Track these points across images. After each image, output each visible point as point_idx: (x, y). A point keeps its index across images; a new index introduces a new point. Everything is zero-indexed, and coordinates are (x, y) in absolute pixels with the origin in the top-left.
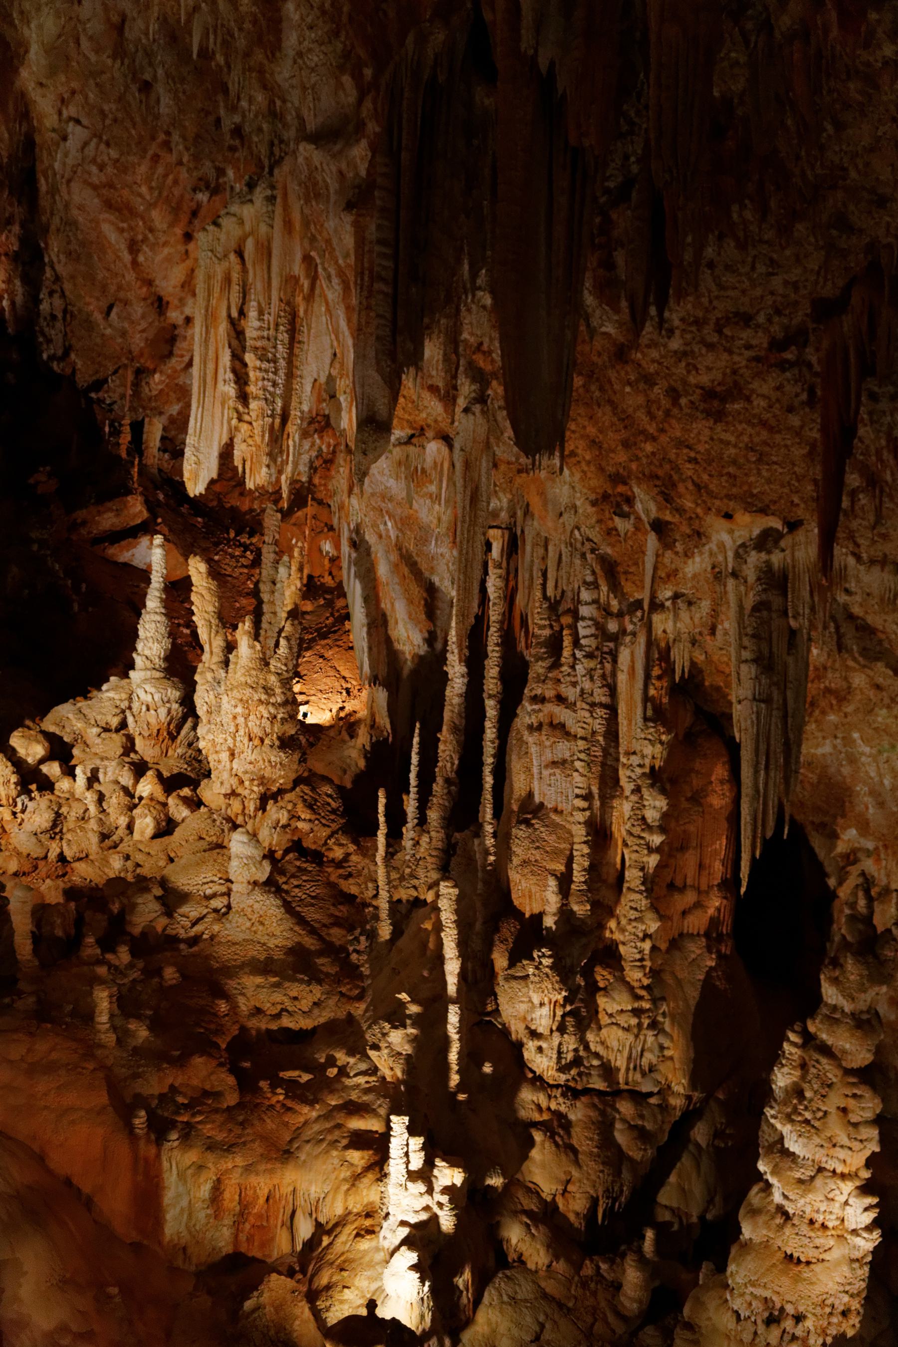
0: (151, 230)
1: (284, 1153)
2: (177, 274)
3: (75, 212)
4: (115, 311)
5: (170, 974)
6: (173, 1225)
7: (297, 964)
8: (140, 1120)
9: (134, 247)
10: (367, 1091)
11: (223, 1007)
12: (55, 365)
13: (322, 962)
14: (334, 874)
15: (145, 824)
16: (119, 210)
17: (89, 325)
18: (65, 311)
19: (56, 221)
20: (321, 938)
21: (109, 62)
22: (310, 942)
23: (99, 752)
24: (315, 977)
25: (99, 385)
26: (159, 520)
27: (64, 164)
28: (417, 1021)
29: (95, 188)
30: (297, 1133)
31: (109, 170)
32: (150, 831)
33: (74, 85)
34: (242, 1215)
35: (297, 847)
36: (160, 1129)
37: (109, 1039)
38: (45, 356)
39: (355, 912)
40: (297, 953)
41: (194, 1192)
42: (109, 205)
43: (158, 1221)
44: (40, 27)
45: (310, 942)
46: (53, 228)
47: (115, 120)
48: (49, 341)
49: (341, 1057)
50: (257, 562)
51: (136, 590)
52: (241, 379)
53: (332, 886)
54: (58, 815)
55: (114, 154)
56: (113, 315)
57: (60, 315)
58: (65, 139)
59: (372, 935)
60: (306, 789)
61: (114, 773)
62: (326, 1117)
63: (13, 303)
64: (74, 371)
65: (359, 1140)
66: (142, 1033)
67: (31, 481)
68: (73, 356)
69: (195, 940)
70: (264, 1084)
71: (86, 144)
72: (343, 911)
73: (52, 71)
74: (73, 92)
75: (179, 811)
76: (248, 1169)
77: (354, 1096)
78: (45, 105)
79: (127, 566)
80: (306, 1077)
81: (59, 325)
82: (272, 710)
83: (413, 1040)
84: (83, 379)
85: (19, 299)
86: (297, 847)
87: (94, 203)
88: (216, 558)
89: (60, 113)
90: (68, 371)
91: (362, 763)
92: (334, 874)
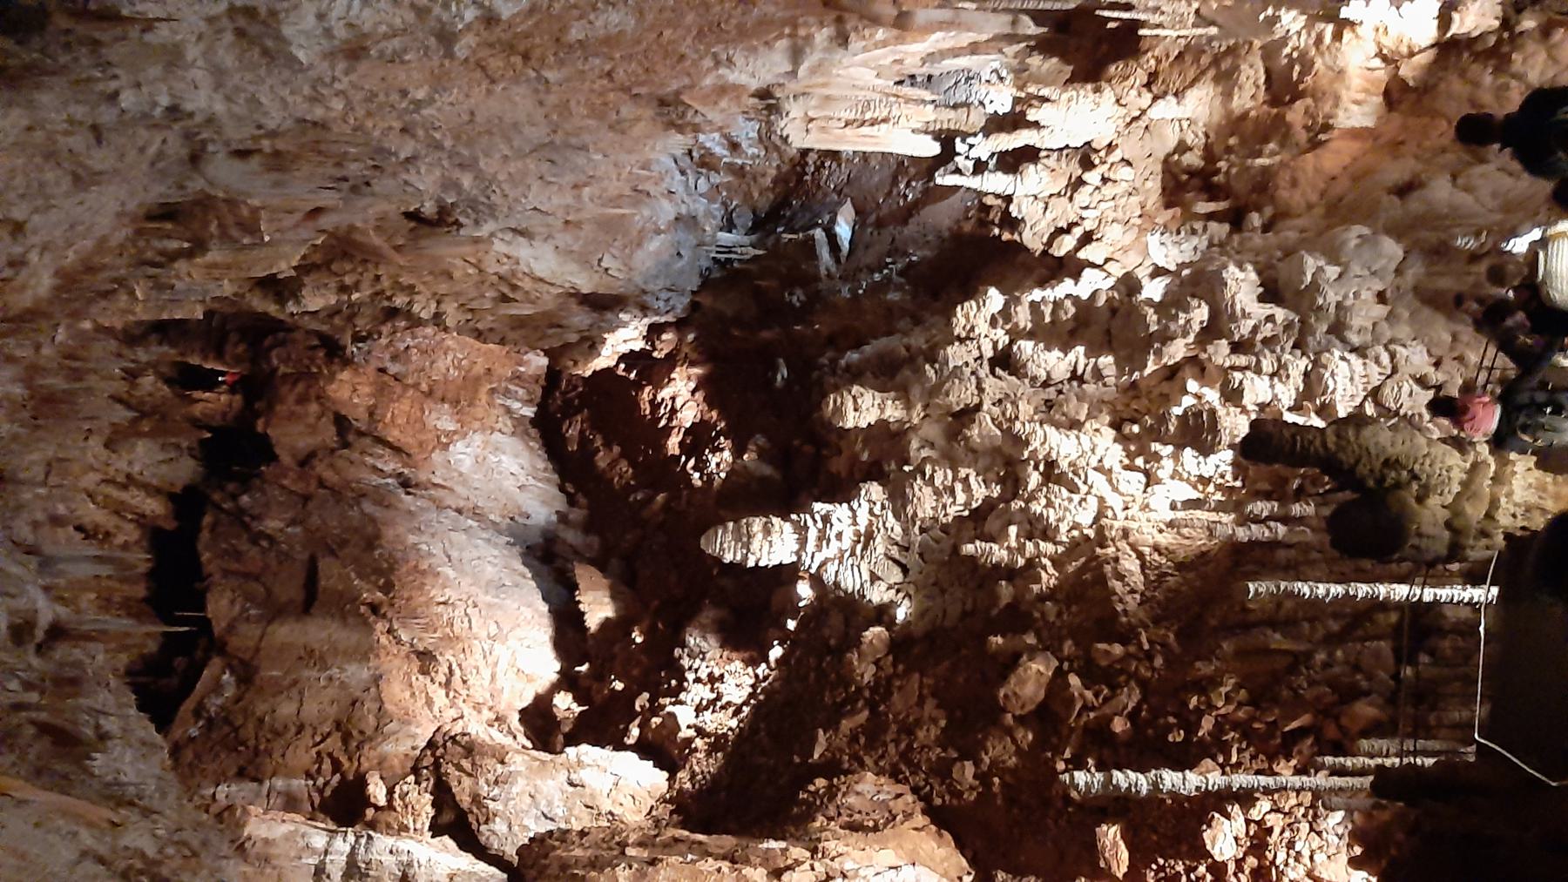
1: (1341, 73)
5: (1232, 141)
6: (1369, 123)
7: (1226, 79)
8: (1322, 137)
9: (658, 232)
10: (1309, 35)
11: (1253, 113)
13: (1225, 65)
14: (1165, 64)
15: (1124, 173)
20: (1208, 69)
22: (1211, 73)
23: (1063, 212)
24: (1235, 68)
28: (1277, 7)
30: (1330, 68)
34: (1366, 91)
35: (1148, 86)
36: (1327, 128)
37: (1278, 158)
39: (1189, 53)
40: (1217, 80)
41: (1356, 110)
43: (1367, 128)
44: (571, 274)
45: (1211, 73)
49: (1287, 50)
50: (835, 155)
53: (1171, 65)
59: (1211, 39)
61: (1083, 196)
62: (1322, 54)
65: (1337, 36)
66: (1272, 146)
69: (1207, 136)
70: (1301, 87)
72: (1188, 58)
75: (1116, 156)
76: (1348, 88)
77: (1311, 42)
80: (1297, 68)
83: (1288, 9)
86: (1148, 86)
91: (1055, 60)
92: (1165, 64)
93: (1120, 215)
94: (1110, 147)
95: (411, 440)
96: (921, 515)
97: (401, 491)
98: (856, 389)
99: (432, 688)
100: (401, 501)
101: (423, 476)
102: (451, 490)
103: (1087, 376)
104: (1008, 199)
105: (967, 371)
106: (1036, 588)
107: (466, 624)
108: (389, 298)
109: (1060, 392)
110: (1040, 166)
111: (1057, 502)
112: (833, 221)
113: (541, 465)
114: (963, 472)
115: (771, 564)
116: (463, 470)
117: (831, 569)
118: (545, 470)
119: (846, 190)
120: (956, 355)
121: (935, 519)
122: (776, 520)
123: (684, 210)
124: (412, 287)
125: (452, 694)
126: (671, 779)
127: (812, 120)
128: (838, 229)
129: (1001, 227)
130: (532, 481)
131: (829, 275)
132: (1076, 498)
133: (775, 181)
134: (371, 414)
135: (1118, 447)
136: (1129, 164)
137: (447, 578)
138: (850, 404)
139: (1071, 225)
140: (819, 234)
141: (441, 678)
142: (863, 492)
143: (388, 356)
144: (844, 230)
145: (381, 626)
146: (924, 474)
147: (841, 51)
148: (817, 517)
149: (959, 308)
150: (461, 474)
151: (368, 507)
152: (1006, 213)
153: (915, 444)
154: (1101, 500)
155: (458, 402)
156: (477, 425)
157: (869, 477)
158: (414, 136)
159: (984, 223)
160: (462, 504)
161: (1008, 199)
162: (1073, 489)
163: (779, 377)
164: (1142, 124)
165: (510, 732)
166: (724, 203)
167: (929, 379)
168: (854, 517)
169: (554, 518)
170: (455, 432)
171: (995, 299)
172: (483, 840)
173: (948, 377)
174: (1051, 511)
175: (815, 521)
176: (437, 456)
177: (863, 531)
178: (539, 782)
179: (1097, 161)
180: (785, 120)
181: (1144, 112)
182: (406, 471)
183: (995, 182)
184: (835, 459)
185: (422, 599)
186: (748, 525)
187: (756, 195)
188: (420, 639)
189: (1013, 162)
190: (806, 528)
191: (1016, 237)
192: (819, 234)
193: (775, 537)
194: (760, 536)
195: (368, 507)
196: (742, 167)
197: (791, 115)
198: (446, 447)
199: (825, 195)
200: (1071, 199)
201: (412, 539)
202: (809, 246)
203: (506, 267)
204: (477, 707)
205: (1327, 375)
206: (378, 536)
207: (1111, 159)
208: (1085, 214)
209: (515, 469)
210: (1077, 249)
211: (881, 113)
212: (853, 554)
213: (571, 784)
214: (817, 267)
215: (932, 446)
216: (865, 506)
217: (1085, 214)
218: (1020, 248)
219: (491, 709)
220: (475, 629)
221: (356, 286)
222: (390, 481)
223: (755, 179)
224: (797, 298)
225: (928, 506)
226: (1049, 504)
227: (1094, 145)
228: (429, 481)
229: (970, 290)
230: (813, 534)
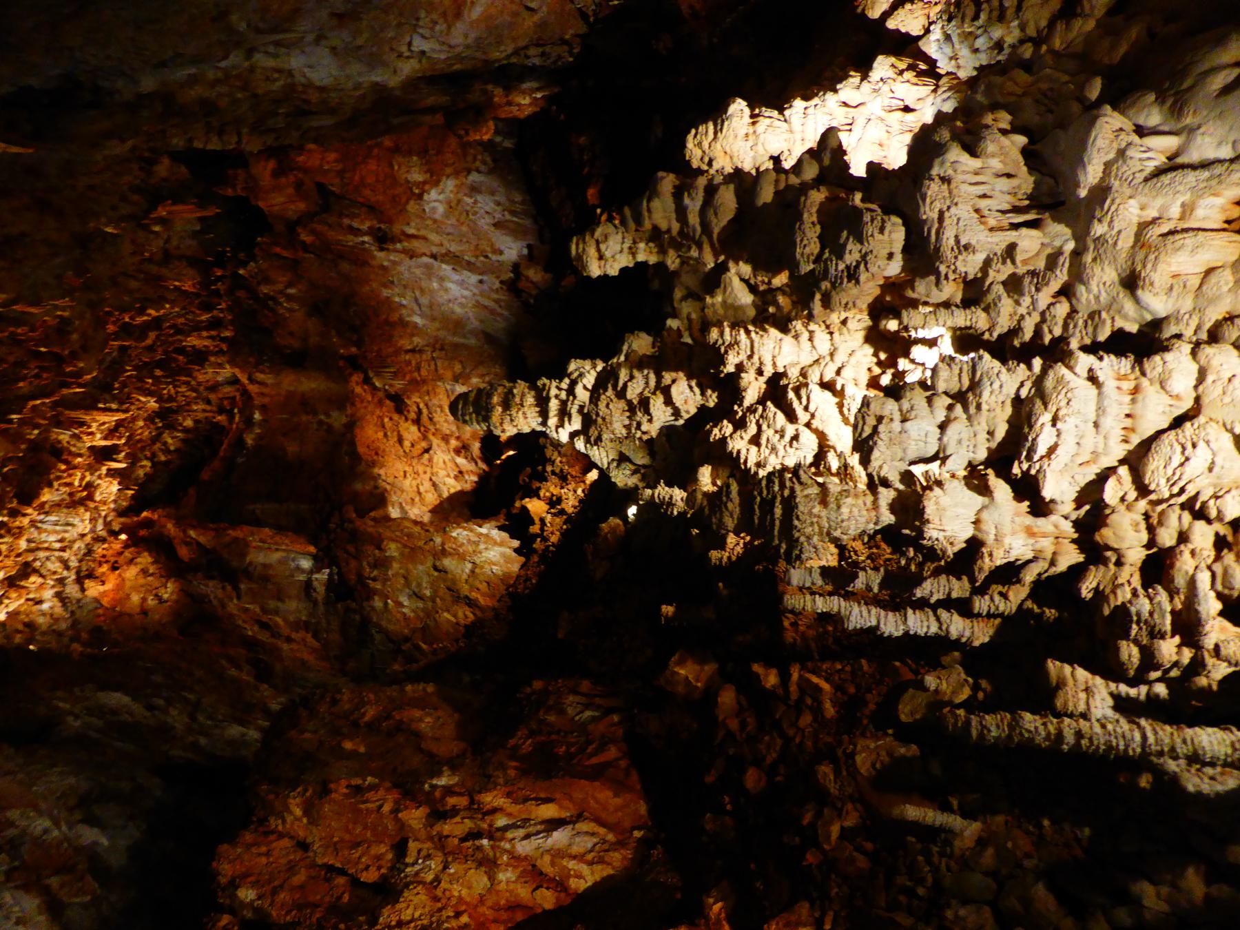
3: (469, 41)
4: (530, 5)
12: (575, 51)
17: (542, 25)
18: (537, 45)
19: (478, 55)
21: (365, 23)
25: (583, 14)
27: (440, 51)
29: (449, 27)
31: (435, 16)
33: (387, 49)
42: (458, 15)
44: (359, 74)
46: (484, 57)
47: (401, 14)
48: (560, 57)
55: (423, 14)
56: (533, 5)
57: (541, 50)
58: (423, 53)
63: (538, 90)
64: (577, 36)
68: (567, 37)
71: (423, 37)
73: (385, 64)
74: (392, 49)
78: (408, 68)
81: (548, 49)
84: (583, 29)
85: (535, 85)
87: (460, 28)
89: (408, 57)
90: (578, 40)
95: (381, 198)
100: (374, 257)
101: (397, 228)
102: (425, 238)
106: (714, 555)
107: (433, 367)
111: (768, 433)
113: (518, 198)
114: (667, 377)
116: (437, 216)
118: (523, 203)
130: (508, 217)
132: (790, 430)
135: (869, 350)
137: (416, 325)
138: (592, 251)
141: (413, 415)
145: (356, 378)
146: (617, 379)
149: (690, 137)
150: (435, 221)
151: (345, 266)
154: (821, 436)
155: (426, 151)
156: (448, 170)
160: (435, 250)
162: (791, 417)
165: (473, 459)
169: (525, 251)
170: (424, 183)
174: (754, 449)
176: (412, 207)
178: (410, 566)
182: (383, 226)
185: (390, 350)
188: (391, 385)
201: (386, 293)
204: (446, 439)
205: (1046, 418)
209: (490, 206)
213: (436, 568)
219: (458, 438)
220: (441, 372)
222: (366, 239)
226: (755, 440)
228: (404, 233)
230: (554, 405)
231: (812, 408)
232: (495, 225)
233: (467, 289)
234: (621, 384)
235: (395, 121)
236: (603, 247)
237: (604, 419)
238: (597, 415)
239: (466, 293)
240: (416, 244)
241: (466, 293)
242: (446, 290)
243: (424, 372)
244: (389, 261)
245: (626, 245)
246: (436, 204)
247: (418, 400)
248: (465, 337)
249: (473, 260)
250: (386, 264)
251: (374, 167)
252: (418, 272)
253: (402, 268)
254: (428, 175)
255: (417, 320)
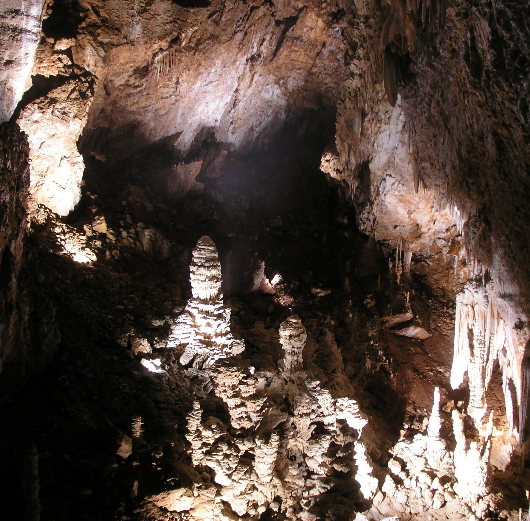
0: (417, 208)
2: (427, 218)
9: (409, 213)
15: (438, 503)
16: (405, 202)
21: (407, 165)
23: (416, 467)
26: (417, 317)
29: (395, 196)
32: (440, 505)
38: (362, 228)
48: (364, 223)
51: (409, 352)
52: (471, 346)
54: (408, 497)
56: (398, 228)
60: (493, 495)
61: (425, 478)
64: (374, 236)
67: (365, 303)
75: (448, 497)
79: (403, 336)
82: (484, 475)
88: (439, 325)
91: (509, 460)
93: (412, 500)
94: (453, 494)
95: (281, 61)
96: (220, 376)
97: (249, 56)
98: (304, 337)
99: (126, 76)
100: (243, 56)
101: (259, 69)
102: (250, 86)
103: (309, 481)
104: (425, 433)
105: (315, 407)
107: (165, 96)
108: (362, 46)
109: (300, 465)
110: (444, 451)
112: (417, 325)
115: (191, 281)
116: (263, 93)
117: (188, 320)
119: (436, 333)
120: (325, 399)
121: (217, 385)
122: (219, 284)
123: (424, 230)
124: (368, 59)
125: (122, 88)
126: (64, 220)
127: (473, 308)
128: (412, 328)
129: (409, 429)
131: (383, 323)
133: (443, 289)
134: (297, 39)
136: (443, 505)
139: (407, 473)
140: (409, 315)
142: (238, 341)
143: (333, 48)
144: (413, 332)
145: (164, 44)
147: (513, 325)
148: (221, 311)
150: (260, 92)
152: (416, 432)
153: (269, 374)
157: (247, 344)
158: (452, 58)
159: (412, 419)
160: (242, 92)
161: (425, 433)
163: (318, 290)
164: (466, 513)
166: (430, 257)
167: (310, 383)
168: (222, 335)
170: (286, 88)
171: (358, 424)
172: (29, 106)
173: (311, 396)
175: (219, 309)
177: (213, 340)
178: (63, 139)
179: (446, 486)
180: (473, 291)
181: (474, 513)
183: (434, 422)
184: (263, 326)
186: (216, 267)
187: (436, 277)
189: (446, 434)
190: (214, 304)
191: (402, 438)
192: (409, 315)
193: (209, 284)
194: (209, 274)
195: (239, 36)
196: (452, 268)
197: (475, 294)
198: (277, 83)
199: (434, 321)
200: (423, 471)
202: (401, 309)
203: (383, 117)
206: (220, 42)
207: (446, 494)
208: (414, 479)
210: (392, 475)
211: (476, 350)
212: (197, 334)
214: (389, 315)
215: (268, 385)
216: (229, 342)
217: (414, 479)
218: (395, 440)
221: (368, 26)
222: (255, 50)
223: (446, 276)
224: (369, 302)
225: (225, 380)
226: (226, 456)
227: (455, 484)
229: (365, 409)
230: (210, 308)
231: (240, 481)
232: (252, 128)
233: (213, 113)
234: (245, 381)
235: (346, 144)
236: (296, 339)
237: (229, 375)
238: (232, 372)
239: (210, 113)
240: (247, 80)
241: (210, 113)
242: (214, 101)
243: (162, 90)
244: (239, 65)
245: (296, 350)
246: (271, 93)
247: (144, 87)
248: (183, 114)
249: (231, 115)
250: (238, 63)
251: (301, 60)
252: (229, 83)
253: (233, 73)
254: (291, 91)
255: (199, 84)
